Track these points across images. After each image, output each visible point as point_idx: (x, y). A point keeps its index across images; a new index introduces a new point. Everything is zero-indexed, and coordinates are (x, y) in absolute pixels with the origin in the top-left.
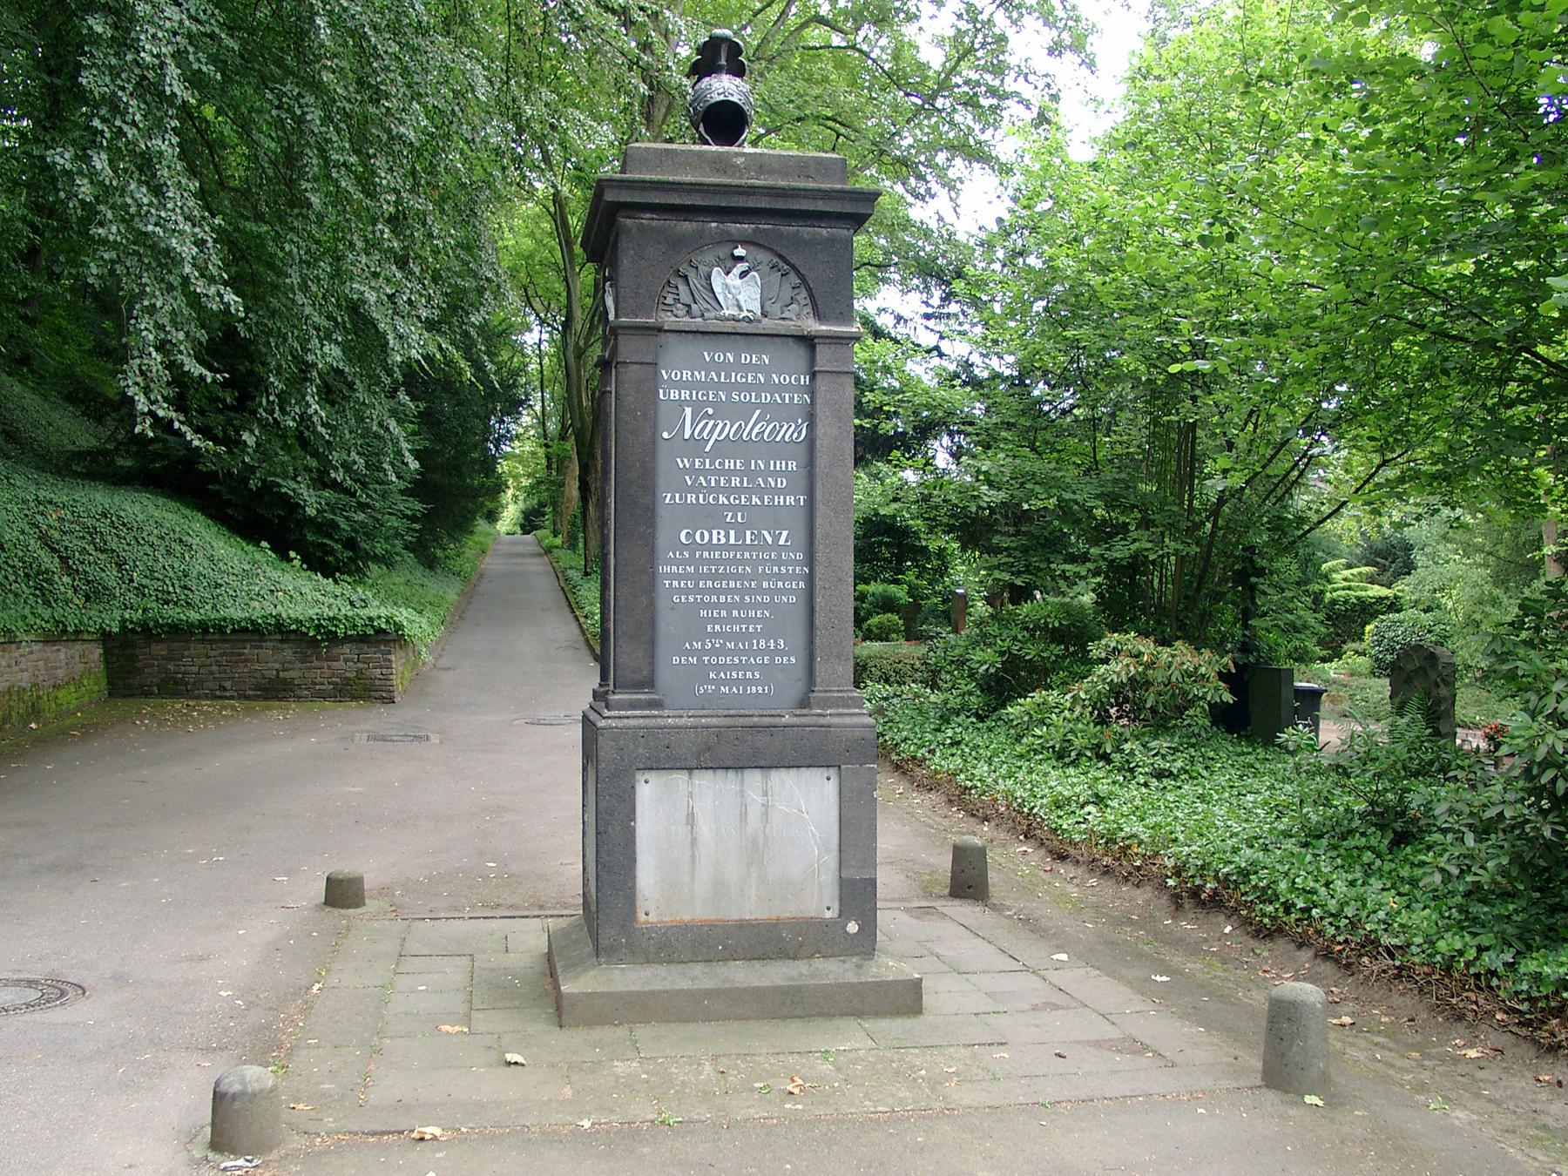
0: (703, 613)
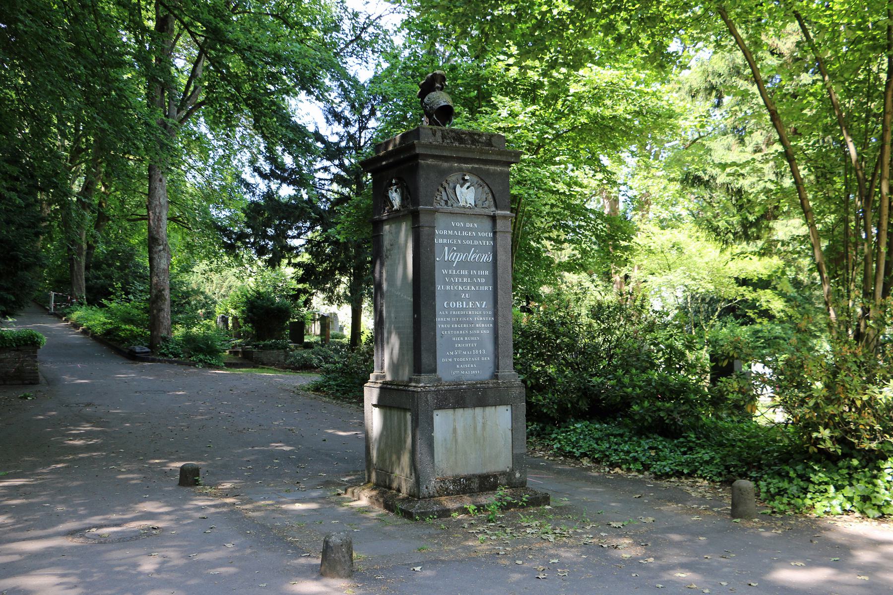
0: (454, 339)
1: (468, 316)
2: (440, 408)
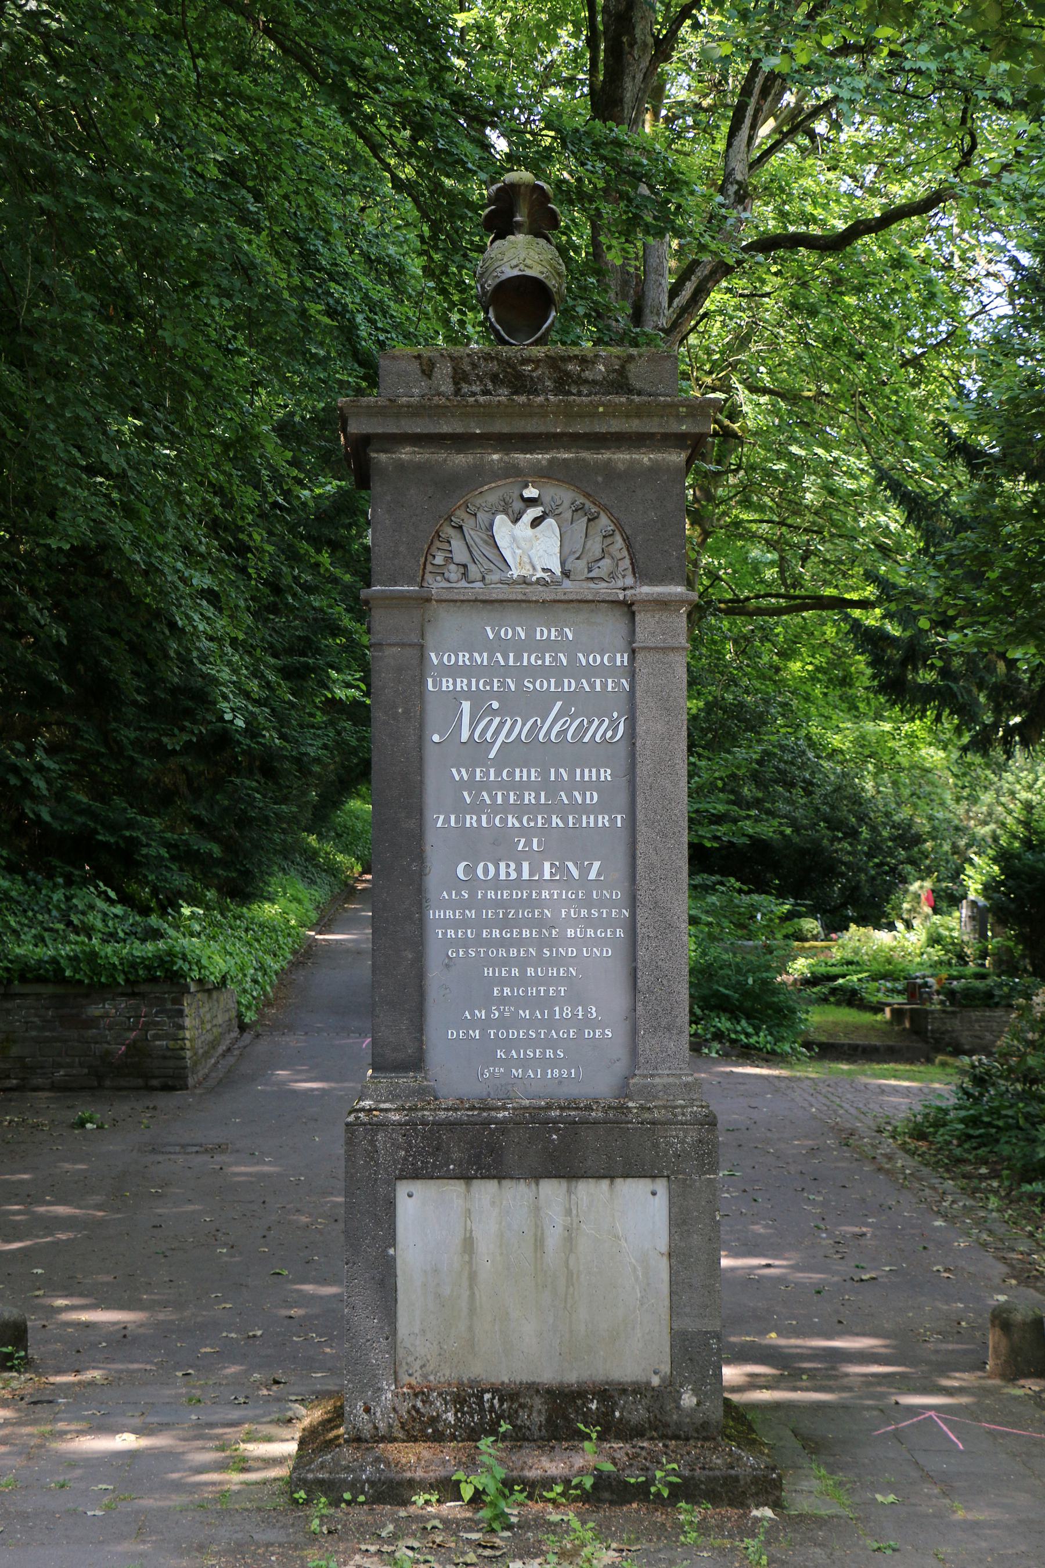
0: (488, 972)
1: (540, 903)
2: (416, 1175)
